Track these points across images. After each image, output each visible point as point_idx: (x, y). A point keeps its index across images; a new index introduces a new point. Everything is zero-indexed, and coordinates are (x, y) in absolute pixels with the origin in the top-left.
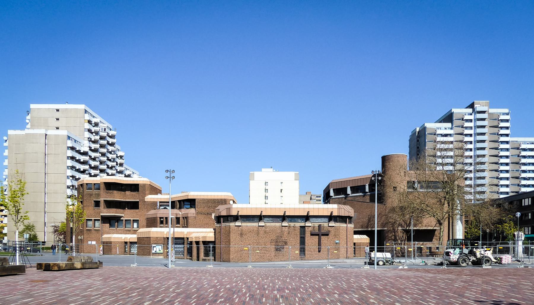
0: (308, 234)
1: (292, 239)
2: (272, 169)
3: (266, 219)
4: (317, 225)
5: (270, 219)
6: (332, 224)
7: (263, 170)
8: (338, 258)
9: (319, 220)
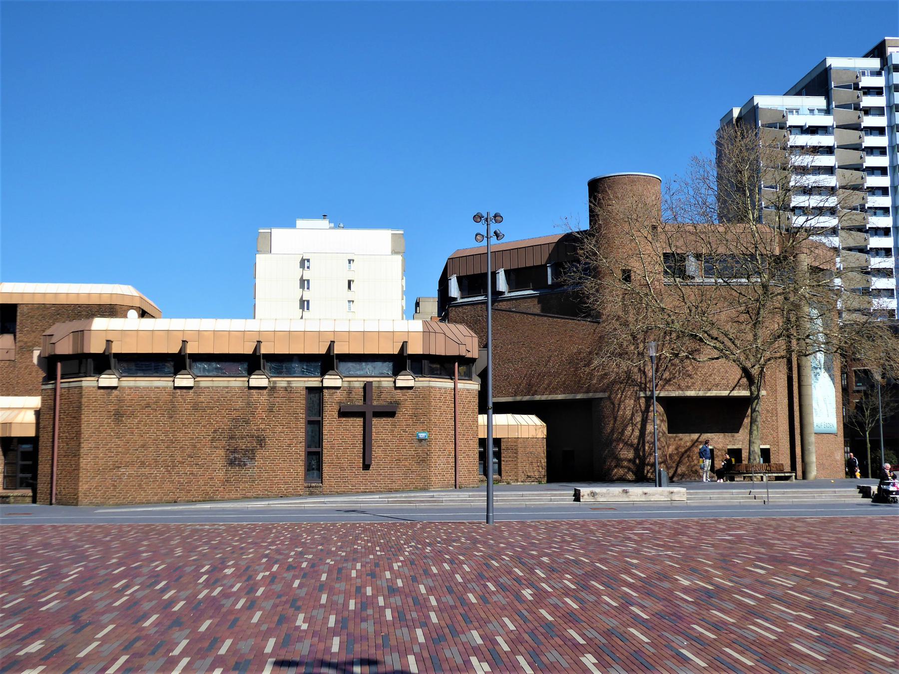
1: (280, 429)
2: (325, 223)
3: (199, 365)
4: (358, 383)
5: (214, 365)
6: (405, 380)
7: (300, 223)
8: (425, 489)
9: (368, 367)
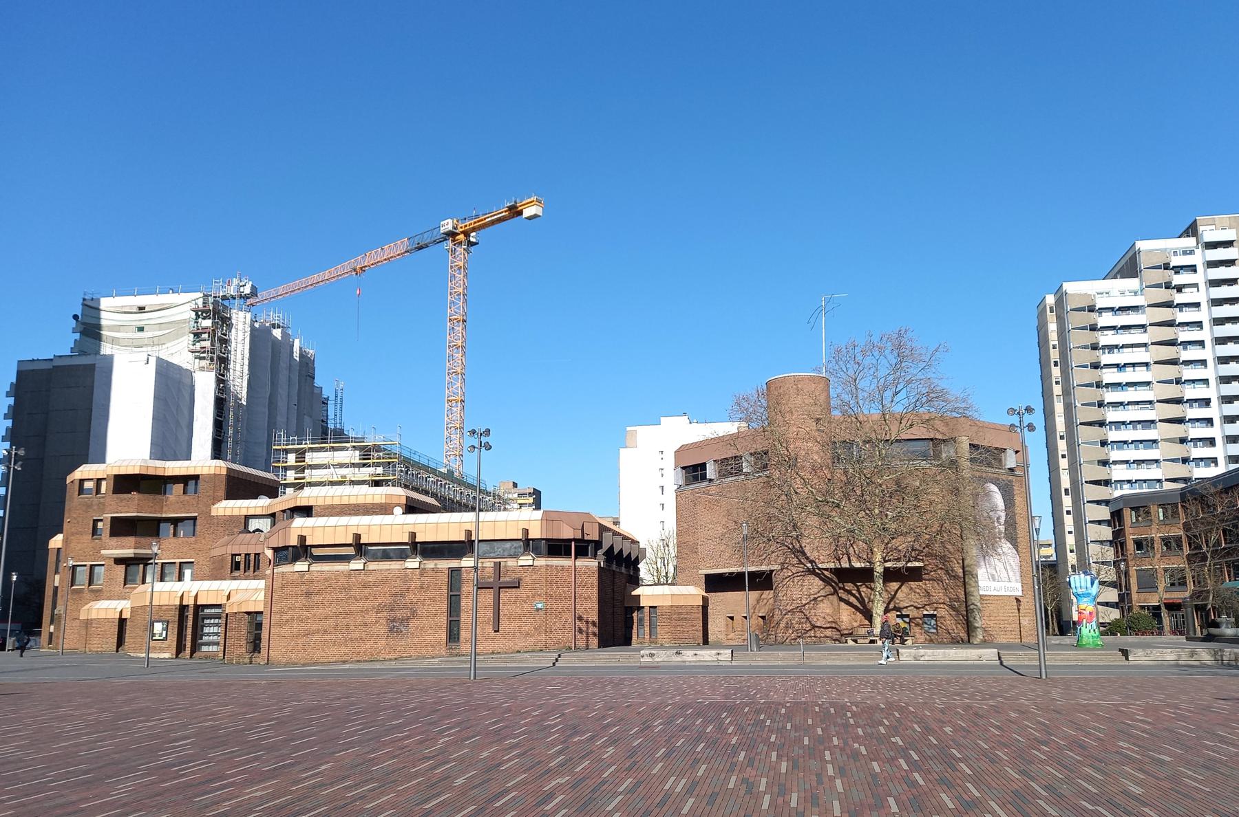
0: (468, 590)
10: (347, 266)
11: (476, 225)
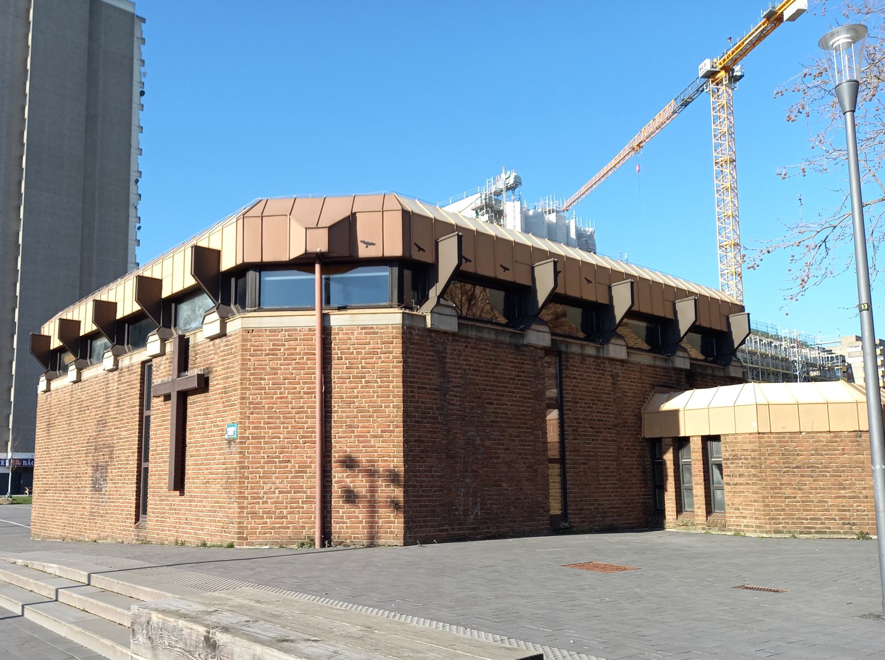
10: (627, 149)
11: (734, 54)
